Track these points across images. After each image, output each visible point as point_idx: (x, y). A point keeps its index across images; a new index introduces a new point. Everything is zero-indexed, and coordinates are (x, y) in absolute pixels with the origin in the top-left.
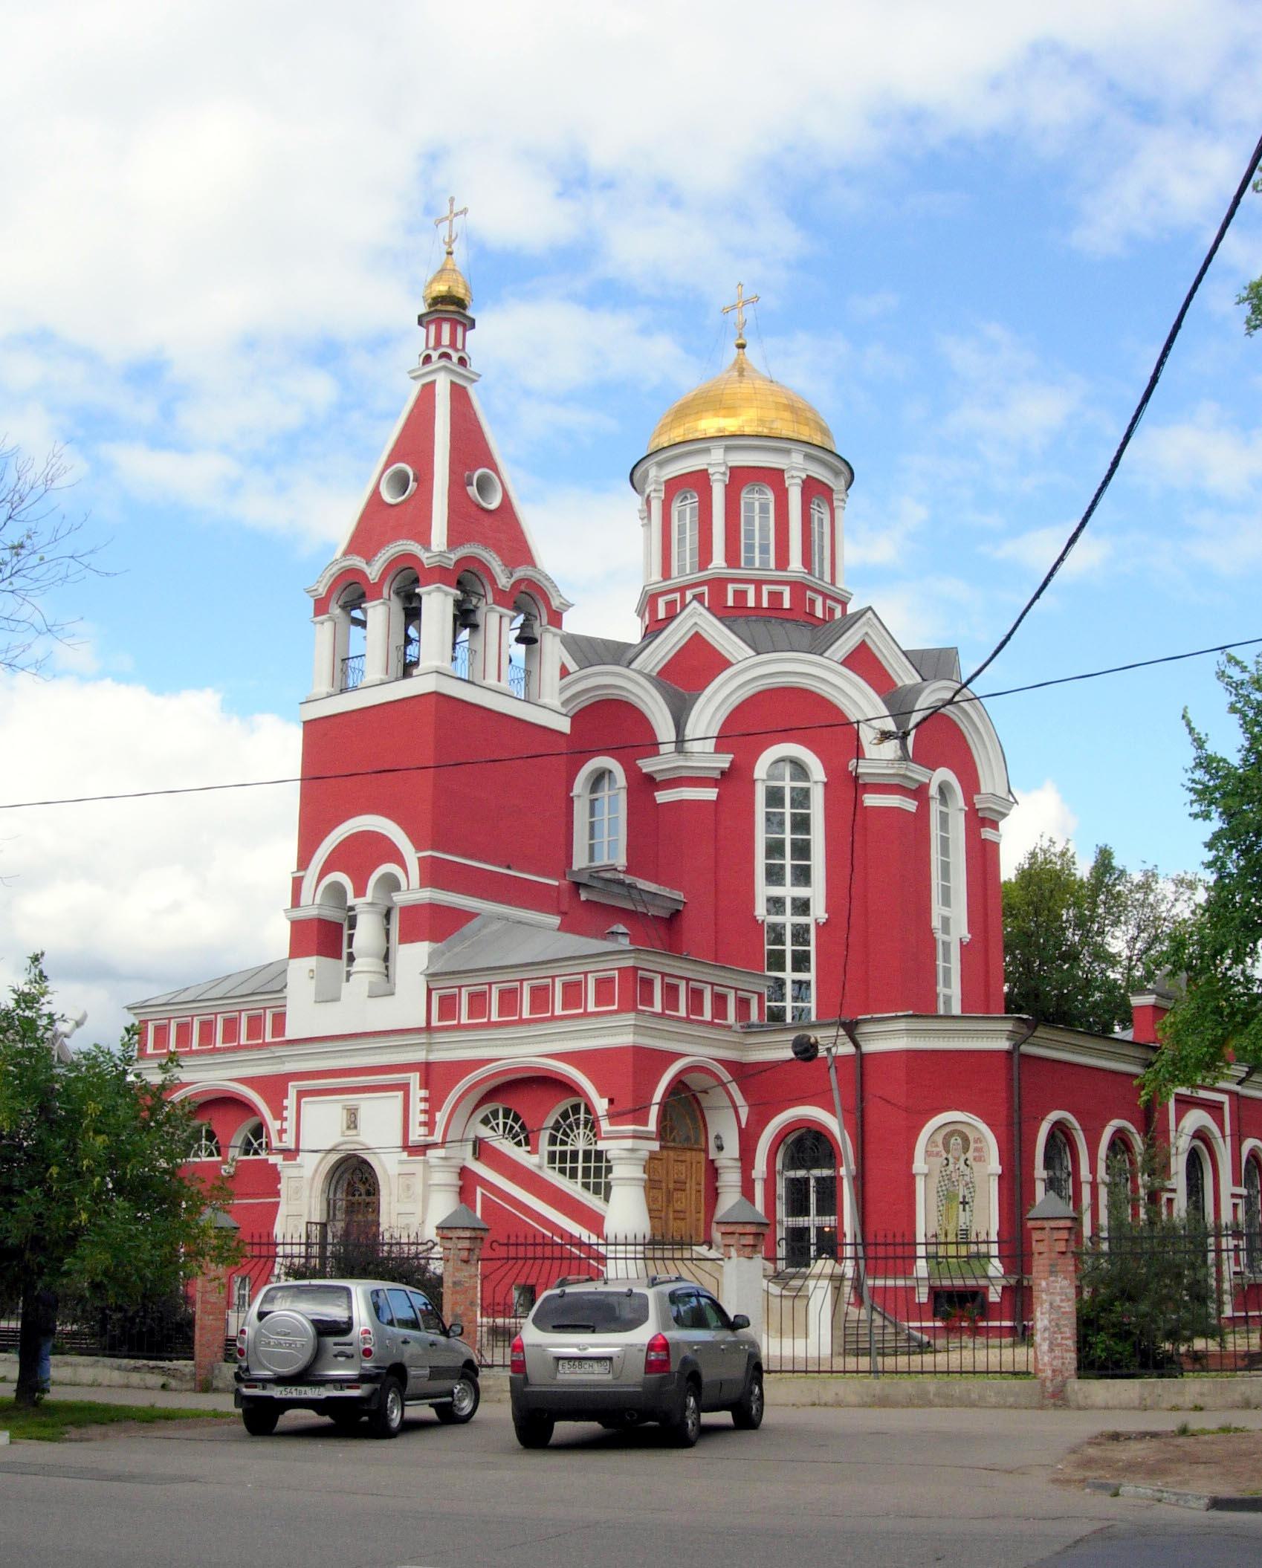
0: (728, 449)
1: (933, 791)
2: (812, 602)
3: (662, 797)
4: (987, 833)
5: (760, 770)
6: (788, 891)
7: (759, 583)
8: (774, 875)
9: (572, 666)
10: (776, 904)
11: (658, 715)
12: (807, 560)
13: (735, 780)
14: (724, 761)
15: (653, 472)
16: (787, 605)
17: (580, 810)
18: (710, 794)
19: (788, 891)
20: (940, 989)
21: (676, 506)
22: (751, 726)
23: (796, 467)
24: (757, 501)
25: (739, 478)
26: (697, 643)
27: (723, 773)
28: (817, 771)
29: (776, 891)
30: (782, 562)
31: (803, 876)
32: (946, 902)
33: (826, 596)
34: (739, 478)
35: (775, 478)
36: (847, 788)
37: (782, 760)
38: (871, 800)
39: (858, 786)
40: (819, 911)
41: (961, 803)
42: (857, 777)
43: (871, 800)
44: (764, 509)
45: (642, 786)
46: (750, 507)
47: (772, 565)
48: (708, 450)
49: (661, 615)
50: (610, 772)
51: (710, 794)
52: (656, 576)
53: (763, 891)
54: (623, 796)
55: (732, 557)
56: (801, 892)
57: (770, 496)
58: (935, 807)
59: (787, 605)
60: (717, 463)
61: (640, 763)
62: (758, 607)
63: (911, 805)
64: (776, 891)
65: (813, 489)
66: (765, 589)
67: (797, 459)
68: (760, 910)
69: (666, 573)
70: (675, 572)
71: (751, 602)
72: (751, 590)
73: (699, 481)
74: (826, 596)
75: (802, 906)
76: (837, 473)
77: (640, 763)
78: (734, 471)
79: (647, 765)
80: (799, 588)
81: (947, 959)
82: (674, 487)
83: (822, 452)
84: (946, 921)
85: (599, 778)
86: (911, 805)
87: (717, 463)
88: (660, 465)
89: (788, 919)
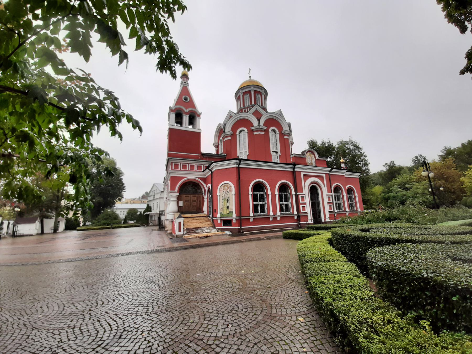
0: (254, 87)
3: (255, 133)
5: (270, 130)
13: (266, 131)
14: (265, 128)
15: (241, 91)
17: (238, 136)
21: (245, 96)
24: (258, 96)
28: (278, 132)
34: (255, 92)
35: (260, 93)
40: (279, 153)
45: (251, 132)
48: (251, 87)
50: (244, 131)
54: (247, 134)
60: (252, 89)
73: (249, 92)
79: (252, 128)
82: (244, 94)
85: (241, 132)
87: (252, 89)
88: (242, 90)
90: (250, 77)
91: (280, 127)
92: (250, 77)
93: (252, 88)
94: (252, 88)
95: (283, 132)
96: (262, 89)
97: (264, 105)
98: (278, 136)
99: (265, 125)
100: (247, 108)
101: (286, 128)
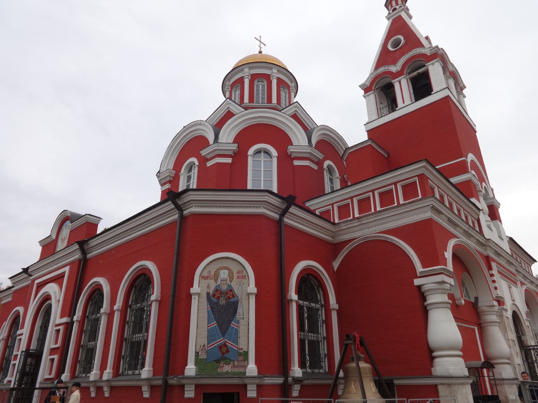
0: (250, 68)
3: (209, 164)
13: (240, 157)
18: (229, 160)
23: (275, 73)
25: (254, 77)
27: (234, 153)
35: (268, 77)
36: (285, 159)
38: (296, 163)
41: (338, 175)
42: (291, 156)
46: (258, 86)
48: (243, 70)
51: (229, 160)
57: (266, 83)
61: (201, 152)
63: (315, 167)
67: (275, 71)
73: (241, 81)
76: (291, 82)
78: (252, 75)
83: (283, 70)
86: (315, 167)
87: (246, 73)
88: (229, 80)
94: (246, 70)
96: (271, 69)
98: (275, 161)
101: (299, 140)
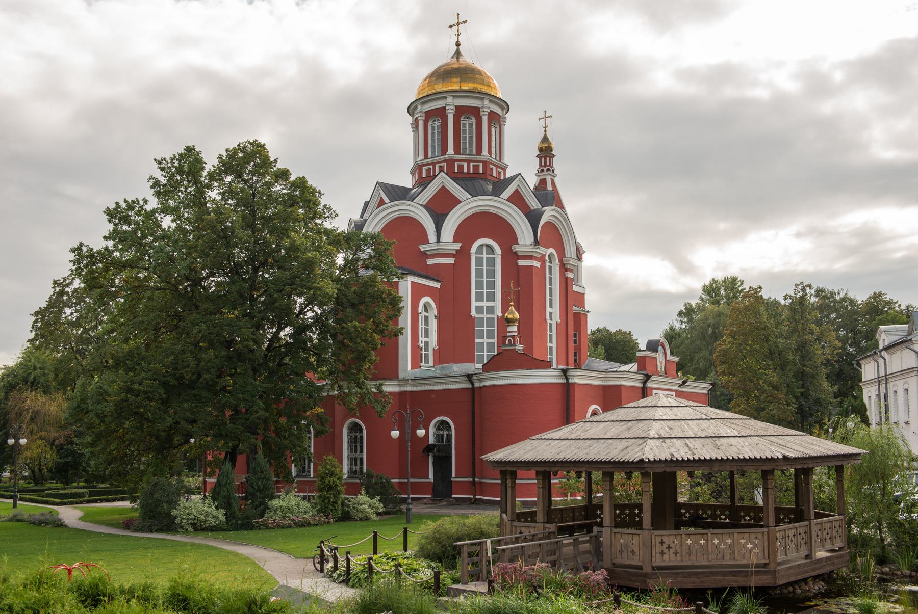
0: (454, 97)
1: (547, 258)
2: (492, 169)
4: (570, 275)
5: (474, 249)
6: (485, 304)
7: (469, 162)
8: (479, 298)
9: (386, 200)
10: (480, 310)
11: (427, 222)
12: (490, 152)
13: (462, 255)
14: (457, 246)
15: (419, 108)
16: (481, 172)
18: (451, 261)
19: (485, 304)
20: (549, 345)
21: (430, 123)
22: (471, 229)
23: (487, 106)
24: (468, 123)
25: (461, 111)
26: (443, 192)
28: (498, 250)
29: (480, 304)
30: (479, 152)
31: (491, 297)
32: (551, 306)
33: (497, 167)
35: (475, 112)
36: (510, 257)
37: (482, 245)
38: (521, 263)
39: (517, 256)
43: (521, 263)
44: (471, 126)
46: (464, 125)
47: (474, 152)
48: (445, 98)
49: (424, 175)
51: (451, 261)
52: (421, 157)
53: (474, 304)
55: (457, 150)
56: (490, 304)
58: (548, 264)
59: (481, 172)
60: (450, 104)
61: (420, 247)
62: (469, 173)
63: (537, 264)
64: (480, 304)
65: (493, 116)
66: (471, 164)
67: (486, 102)
68: (473, 313)
69: (426, 156)
70: (430, 156)
71: (465, 171)
72: (465, 164)
73: (441, 113)
74: (497, 167)
75: (491, 310)
76: (503, 109)
77: (420, 247)
80: (485, 163)
81: (551, 331)
82: (429, 115)
84: (551, 314)
86: (537, 264)
87: (450, 104)
88: (423, 104)
89: (485, 316)
90: (458, 44)
91: (506, 235)
92: (458, 44)
93: (450, 100)
94: (450, 100)
95: (516, 248)
96: (482, 99)
97: (485, 152)
99: (455, 240)
100: (434, 164)
